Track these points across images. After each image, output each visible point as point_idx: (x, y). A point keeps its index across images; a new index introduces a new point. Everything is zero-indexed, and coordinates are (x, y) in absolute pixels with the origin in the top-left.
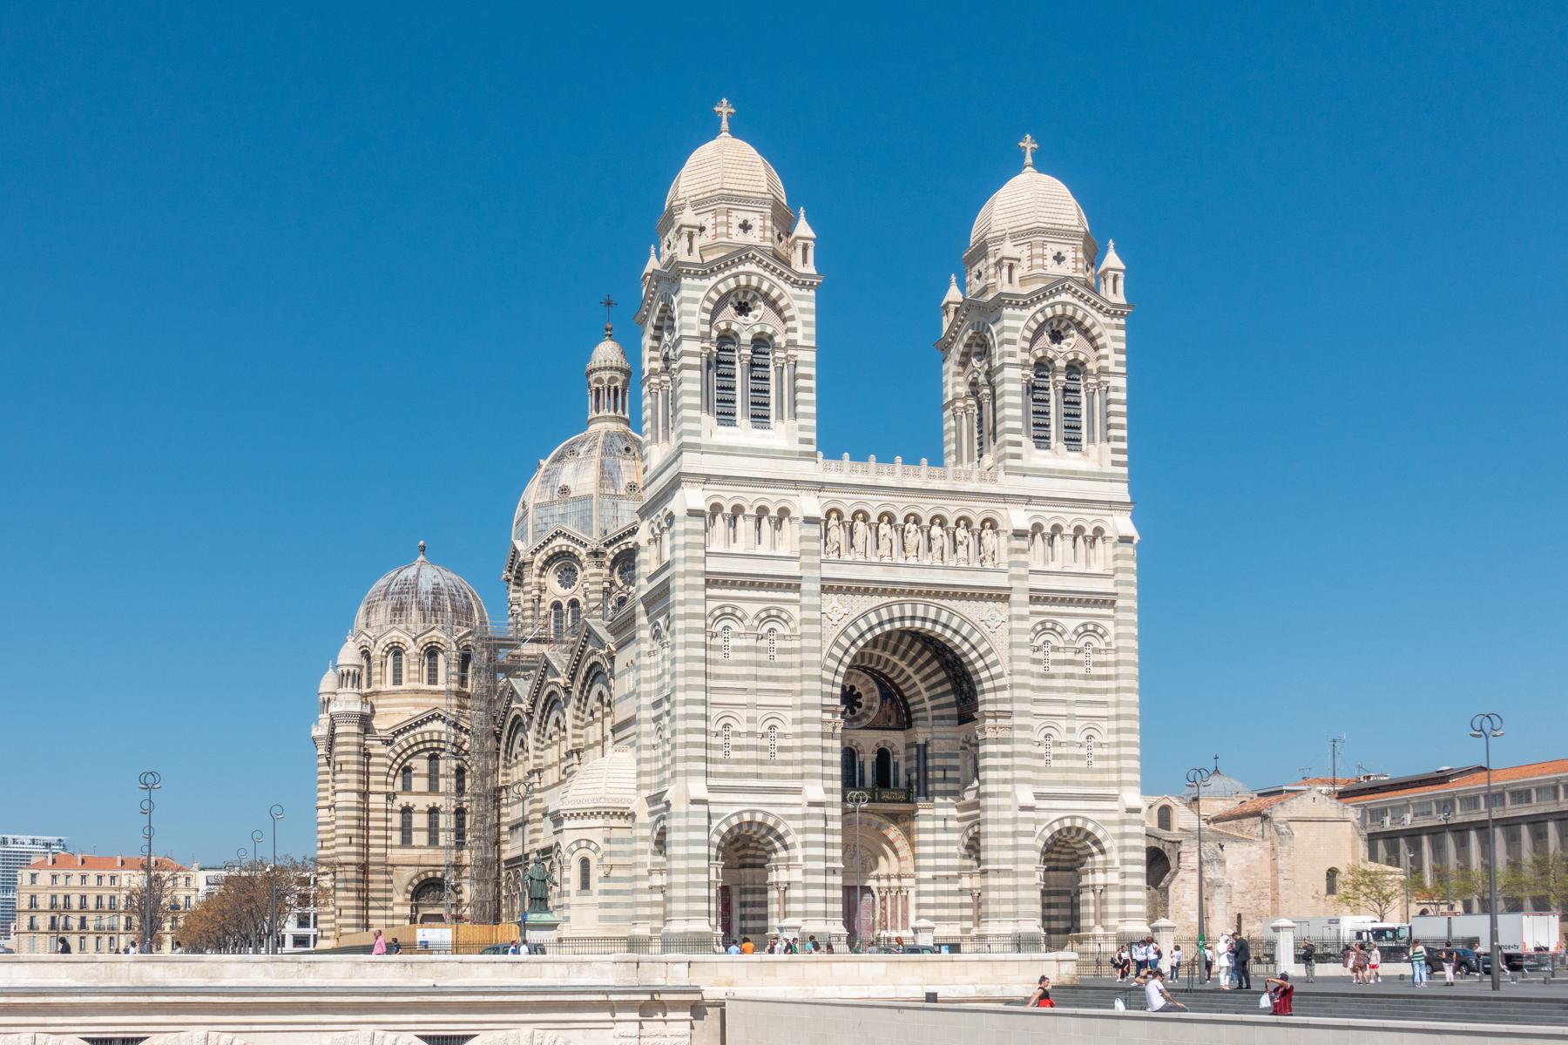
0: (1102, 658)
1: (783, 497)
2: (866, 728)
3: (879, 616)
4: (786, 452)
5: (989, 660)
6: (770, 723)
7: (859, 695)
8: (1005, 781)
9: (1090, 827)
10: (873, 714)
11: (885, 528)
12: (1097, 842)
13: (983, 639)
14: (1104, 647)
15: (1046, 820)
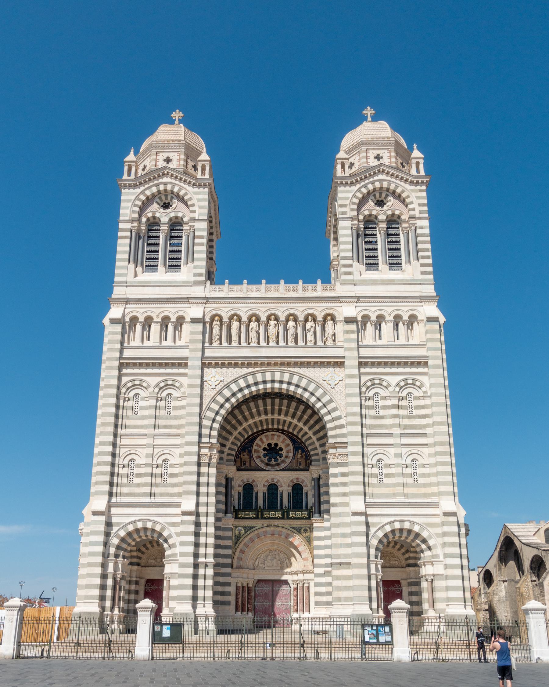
0: (421, 403)
1: (180, 309)
2: (283, 470)
3: (246, 381)
4: (184, 282)
5: (330, 407)
6: (164, 457)
7: (281, 449)
8: (345, 494)
9: (416, 529)
10: (288, 461)
11: (254, 325)
12: (424, 541)
13: (325, 393)
14: (422, 395)
15: (379, 523)
